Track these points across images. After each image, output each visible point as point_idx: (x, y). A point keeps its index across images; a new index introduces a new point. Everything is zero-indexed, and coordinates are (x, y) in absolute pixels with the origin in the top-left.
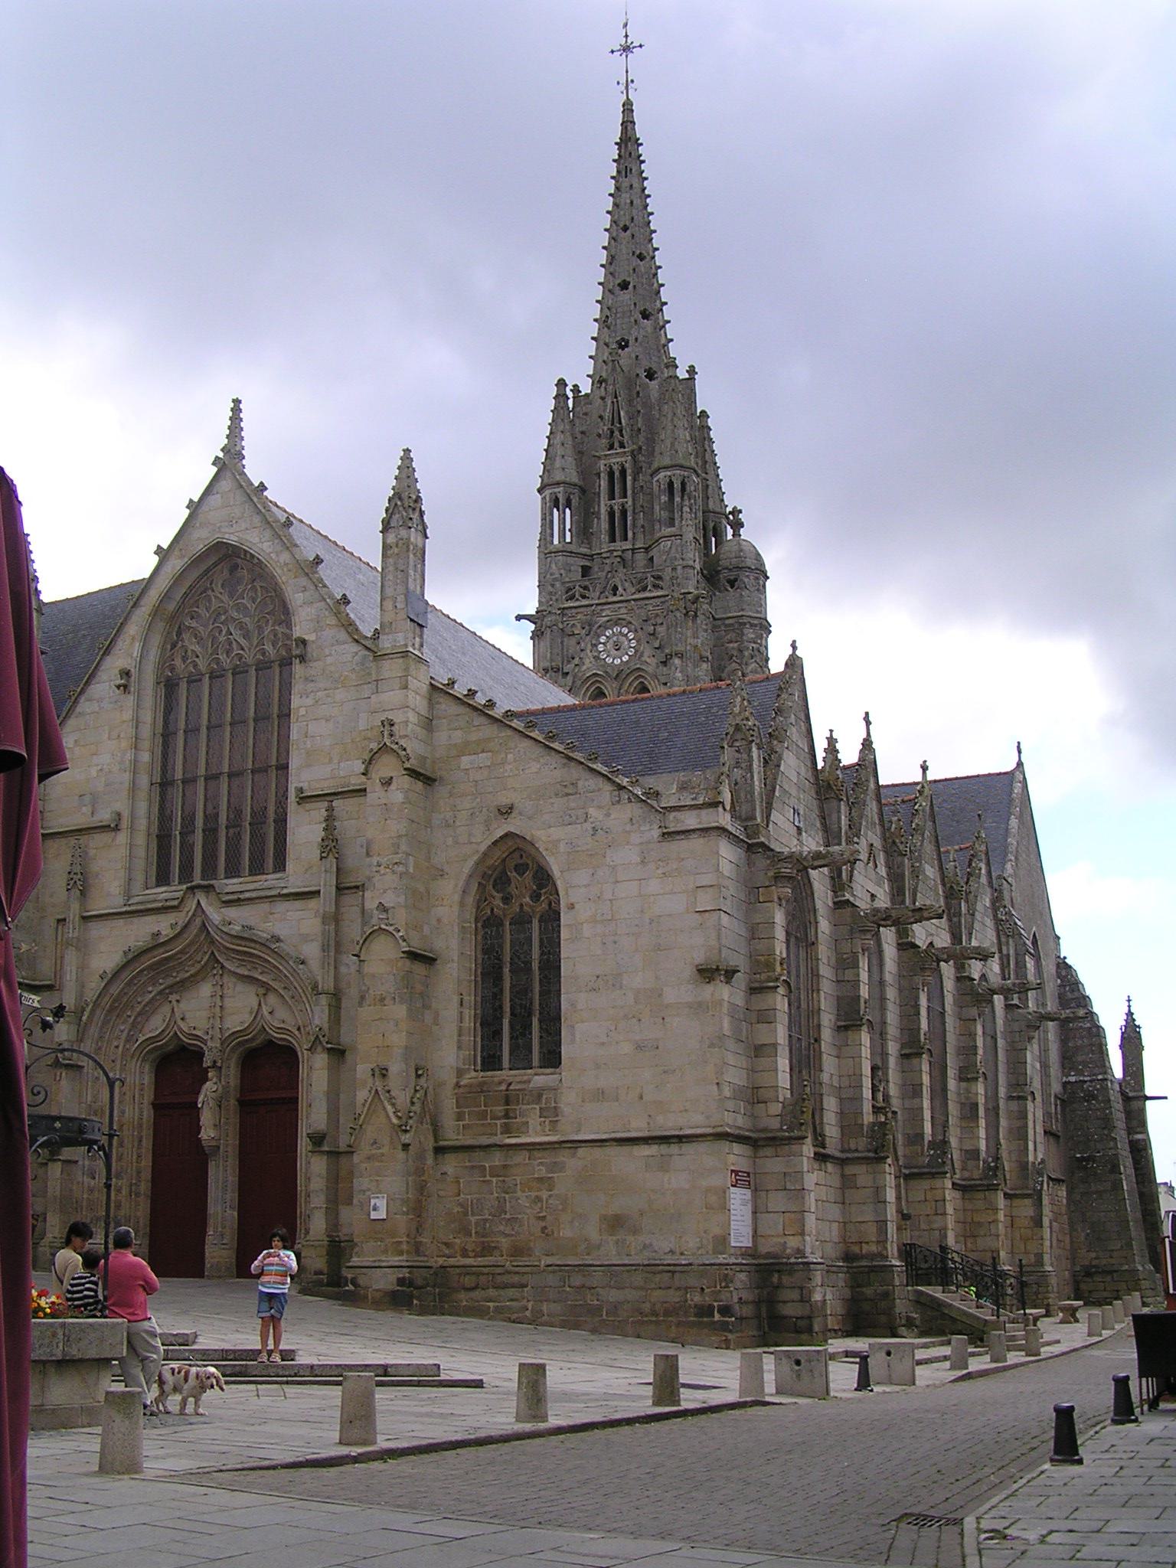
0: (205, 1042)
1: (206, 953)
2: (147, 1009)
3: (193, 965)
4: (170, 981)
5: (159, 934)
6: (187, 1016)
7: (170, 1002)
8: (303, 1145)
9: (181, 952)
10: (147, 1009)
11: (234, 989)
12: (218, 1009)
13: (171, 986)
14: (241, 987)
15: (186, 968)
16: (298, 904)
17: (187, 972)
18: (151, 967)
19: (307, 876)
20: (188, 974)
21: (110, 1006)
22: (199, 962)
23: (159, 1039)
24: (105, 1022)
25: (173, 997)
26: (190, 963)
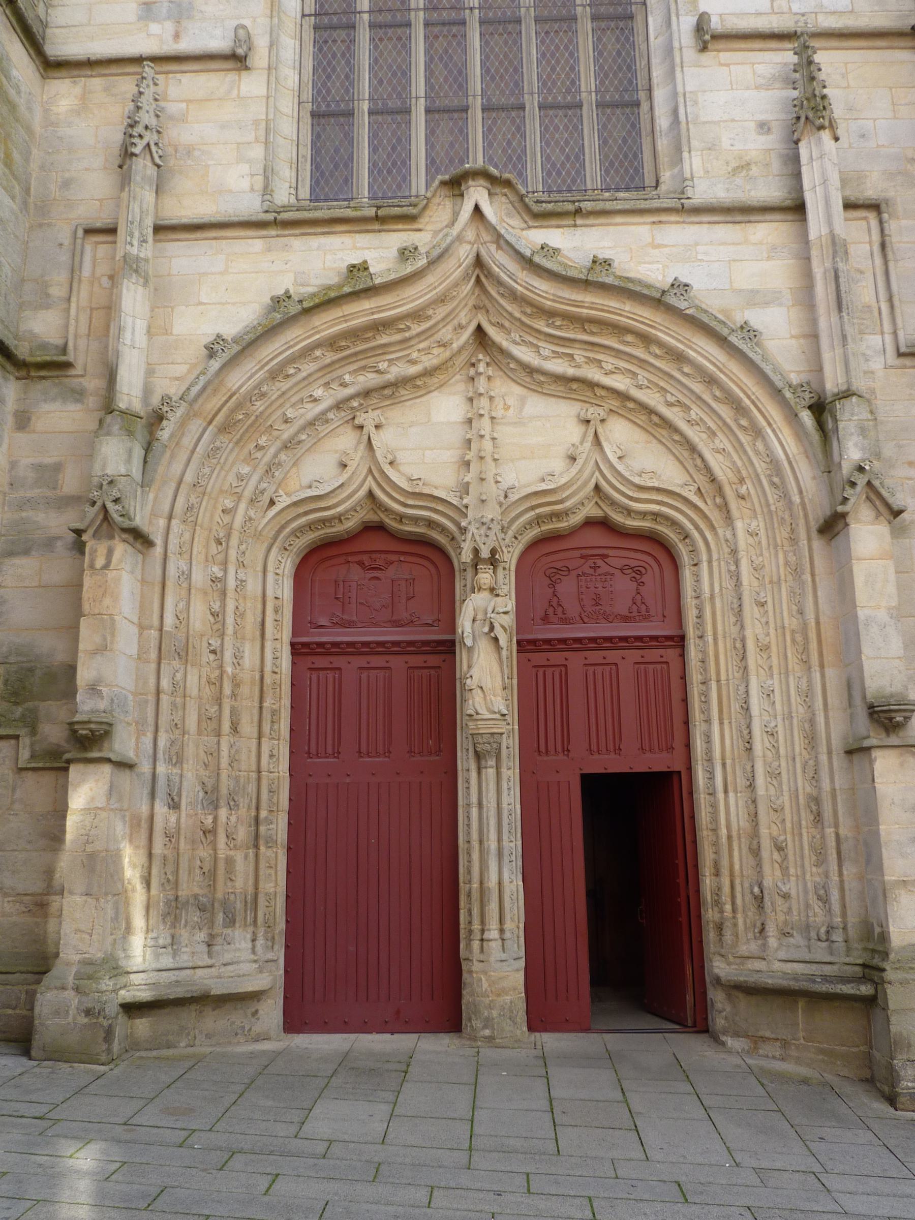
0: (462, 511)
1: (461, 327)
2: (303, 437)
3: (427, 351)
4: (369, 379)
5: (364, 267)
6: (401, 457)
7: (361, 427)
8: (511, 744)
9: (417, 315)
10: (303, 437)
11: (521, 410)
12: (487, 445)
13: (367, 393)
14: (537, 405)
15: (415, 355)
16: (724, 232)
17: (413, 362)
18: (332, 343)
19: (739, 181)
20: (413, 370)
21: (227, 417)
22: (443, 345)
23: (323, 504)
24: (211, 454)
25: (368, 419)
26: (421, 346)
